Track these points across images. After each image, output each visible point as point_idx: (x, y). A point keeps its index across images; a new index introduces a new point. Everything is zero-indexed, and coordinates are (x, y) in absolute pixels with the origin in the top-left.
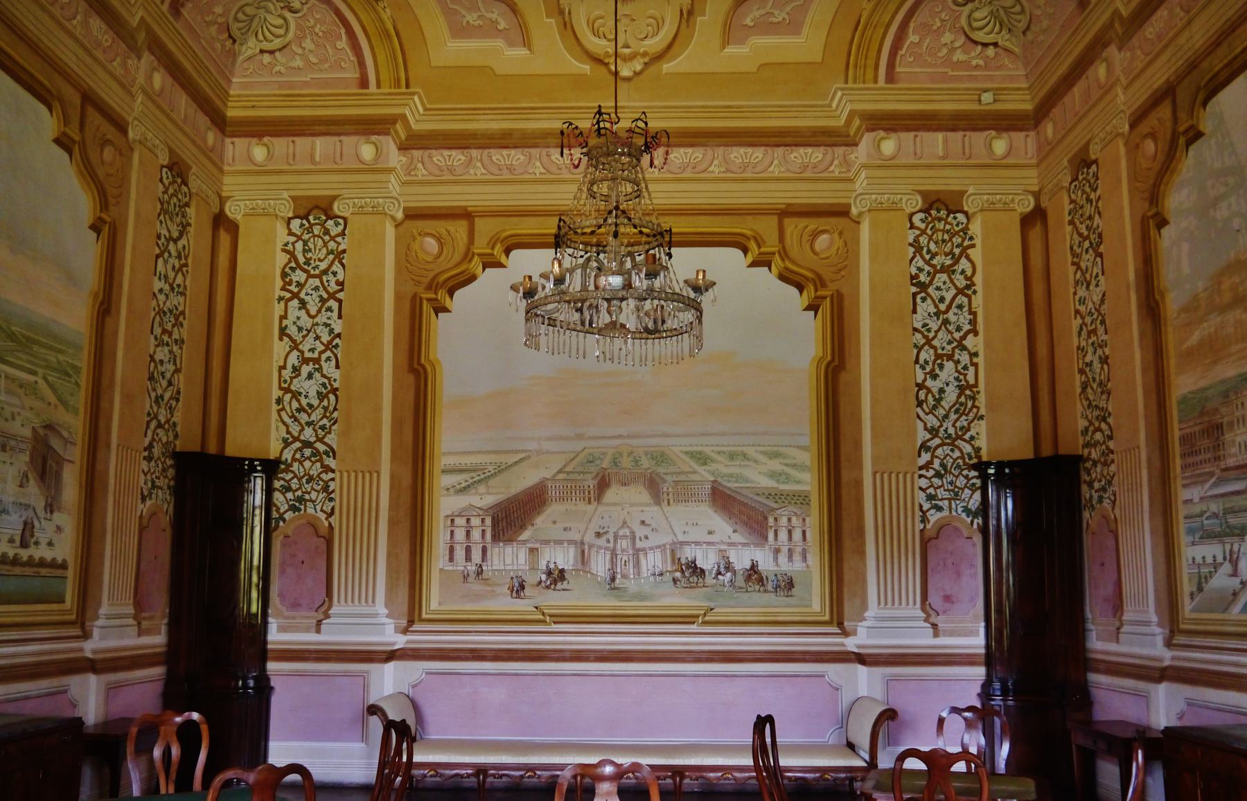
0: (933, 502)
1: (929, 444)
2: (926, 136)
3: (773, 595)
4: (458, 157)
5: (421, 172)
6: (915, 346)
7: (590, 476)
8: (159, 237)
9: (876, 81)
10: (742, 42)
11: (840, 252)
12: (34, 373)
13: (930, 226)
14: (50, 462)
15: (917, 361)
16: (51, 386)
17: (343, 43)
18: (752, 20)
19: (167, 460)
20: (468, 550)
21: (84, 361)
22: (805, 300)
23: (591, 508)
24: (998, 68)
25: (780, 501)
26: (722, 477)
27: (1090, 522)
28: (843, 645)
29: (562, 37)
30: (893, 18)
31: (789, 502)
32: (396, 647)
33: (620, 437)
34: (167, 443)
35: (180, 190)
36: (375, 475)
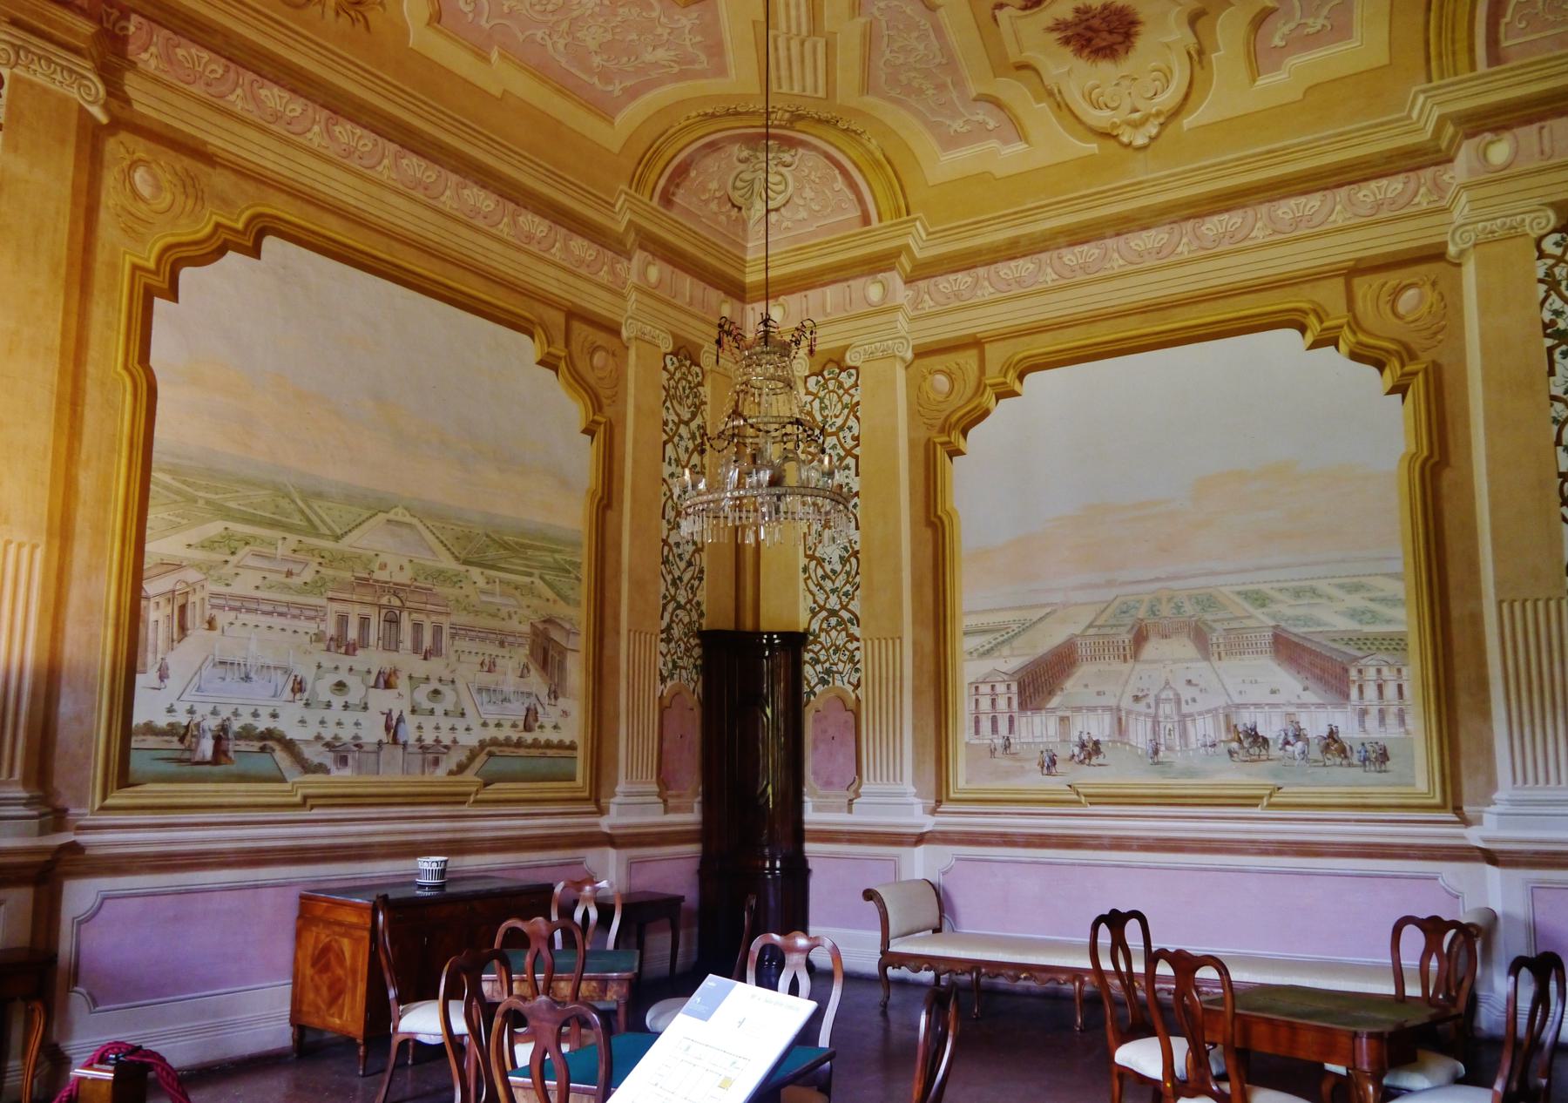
3: (1357, 772)
4: (964, 278)
6: (1555, 421)
7: (1123, 630)
8: (666, 423)
9: (1473, 67)
10: (1276, 67)
11: (1434, 310)
12: (530, 575)
14: (551, 652)
16: (550, 585)
17: (840, 183)
18: (1282, 39)
19: (691, 640)
20: (994, 720)
21: (584, 557)
22: (1388, 380)
23: (1126, 667)
25: (1363, 647)
26: (1287, 620)
32: (925, 830)
33: (1158, 579)
34: (690, 623)
35: (689, 372)
36: (898, 641)
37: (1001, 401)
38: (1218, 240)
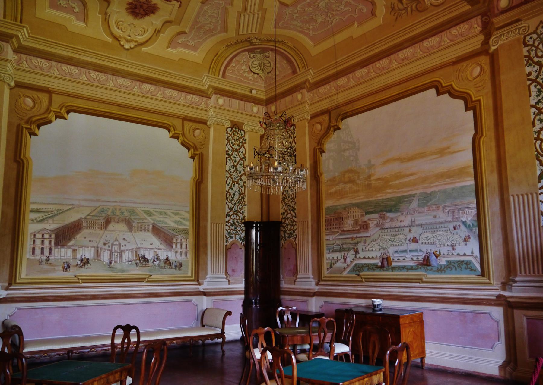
0: (230, 235)
1: (229, 213)
2: (233, 100)
3: (173, 270)
5: (25, 66)
9: (218, 76)
10: (175, 48)
13: (233, 133)
15: (227, 183)
20: (42, 250)
23: (101, 232)
24: (257, 82)
25: (178, 232)
27: (284, 244)
28: (199, 289)
30: (229, 56)
31: (182, 233)
37: (57, 119)
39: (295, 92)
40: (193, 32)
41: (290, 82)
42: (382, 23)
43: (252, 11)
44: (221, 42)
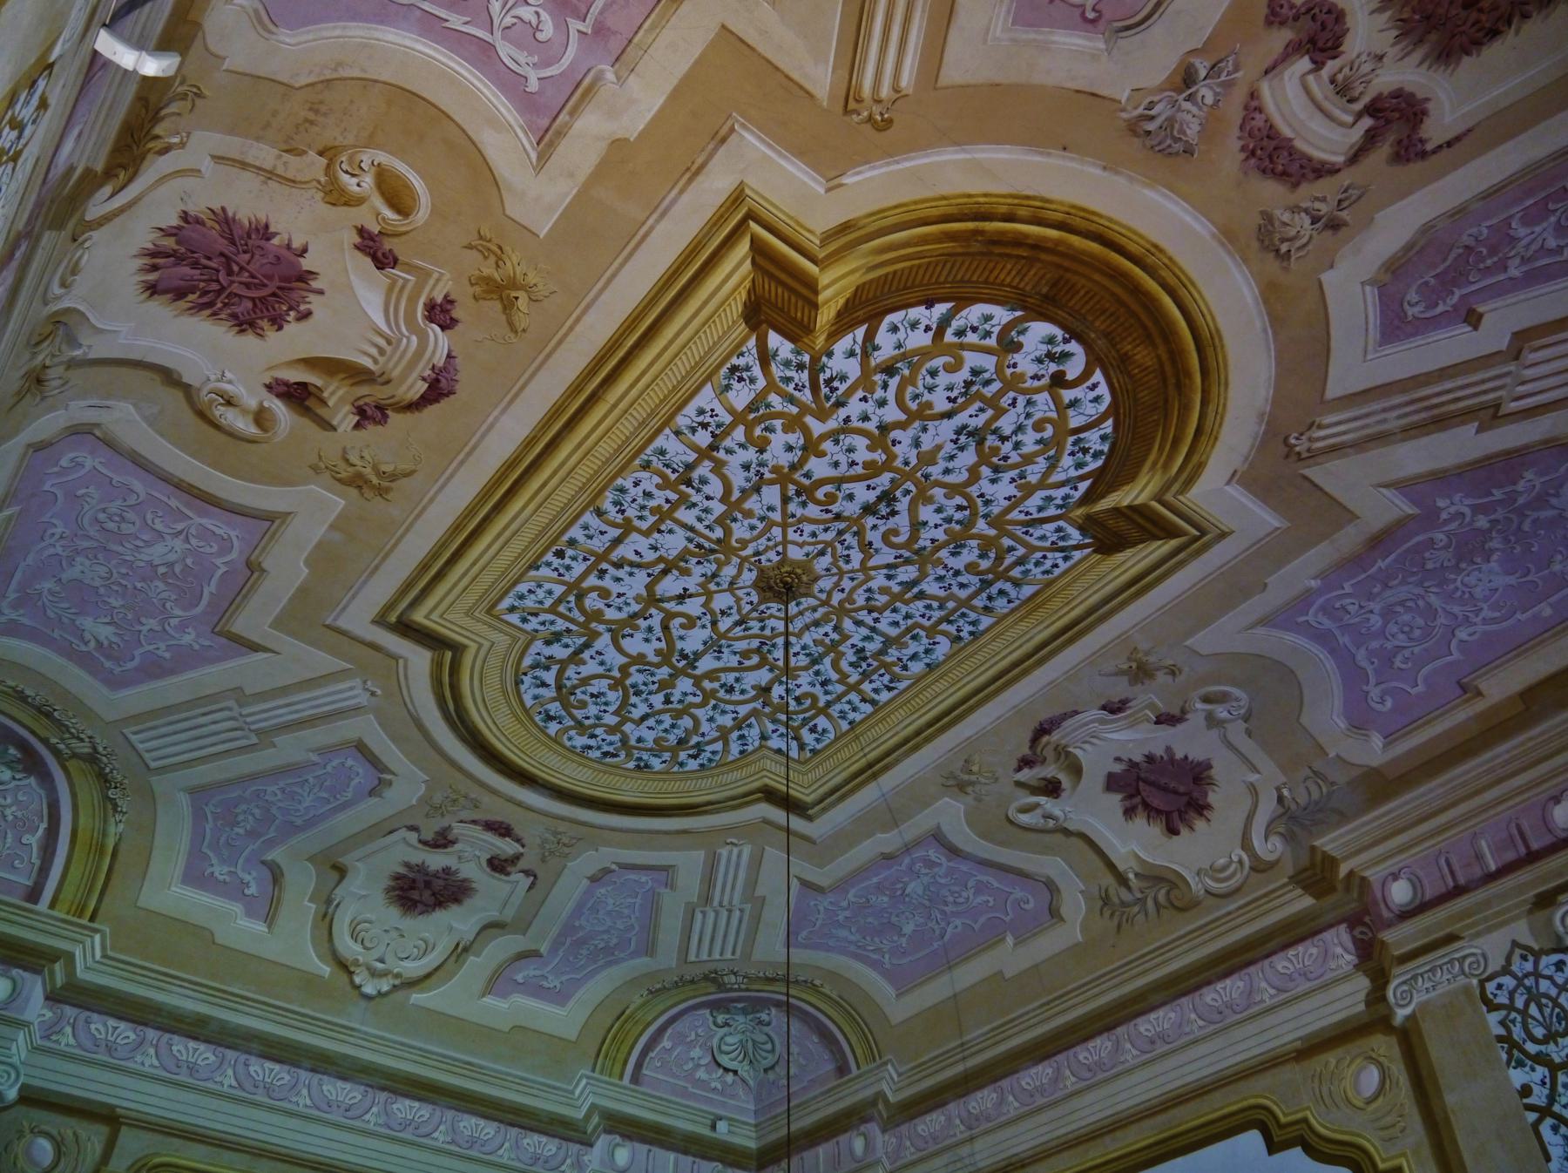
2: (658, 1152)
4: (126, 1032)
5: (67, 1039)
9: (621, 1077)
10: (504, 995)
17: (34, 840)
24: (733, 1097)
29: (315, 927)
30: (655, 1019)
38: (406, 1125)
39: (846, 1131)
40: (561, 953)
41: (830, 1100)
42: (1080, 938)
43: (725, 903)
44: (634, 982)
